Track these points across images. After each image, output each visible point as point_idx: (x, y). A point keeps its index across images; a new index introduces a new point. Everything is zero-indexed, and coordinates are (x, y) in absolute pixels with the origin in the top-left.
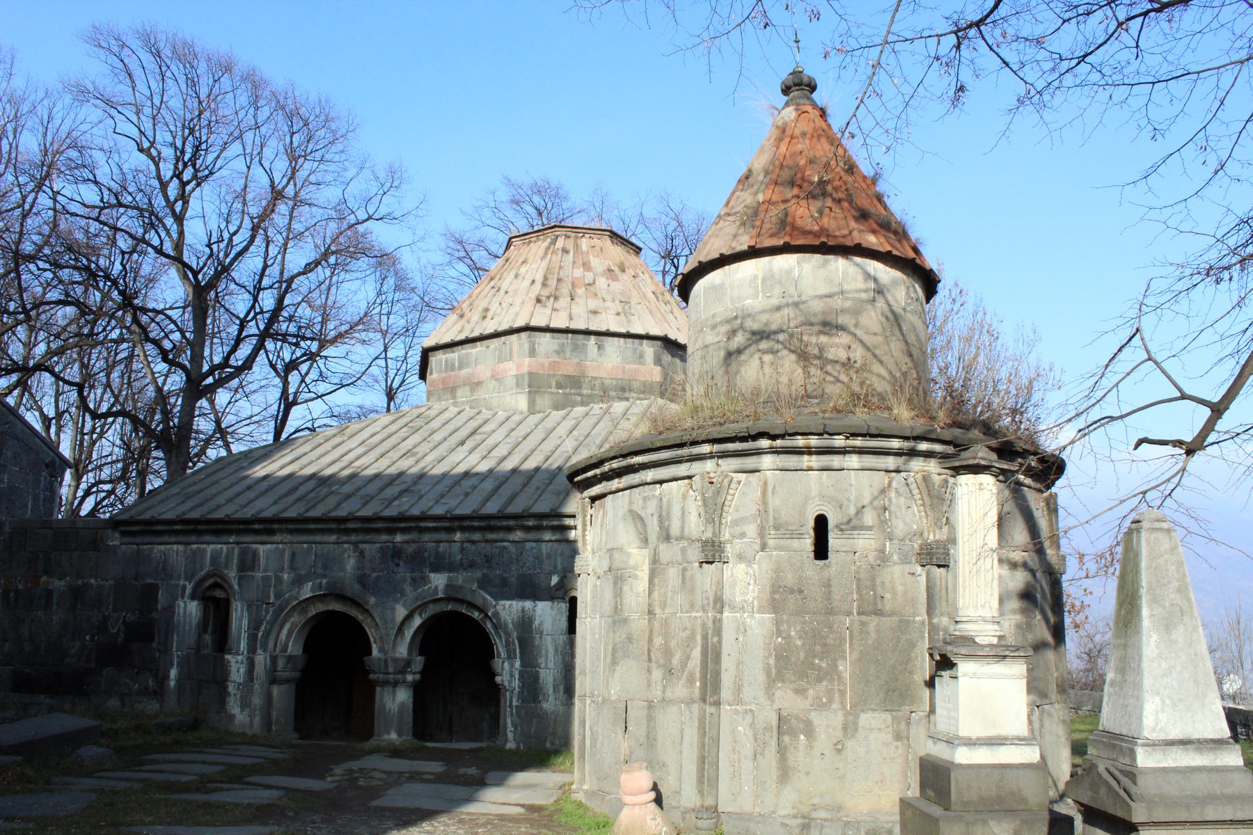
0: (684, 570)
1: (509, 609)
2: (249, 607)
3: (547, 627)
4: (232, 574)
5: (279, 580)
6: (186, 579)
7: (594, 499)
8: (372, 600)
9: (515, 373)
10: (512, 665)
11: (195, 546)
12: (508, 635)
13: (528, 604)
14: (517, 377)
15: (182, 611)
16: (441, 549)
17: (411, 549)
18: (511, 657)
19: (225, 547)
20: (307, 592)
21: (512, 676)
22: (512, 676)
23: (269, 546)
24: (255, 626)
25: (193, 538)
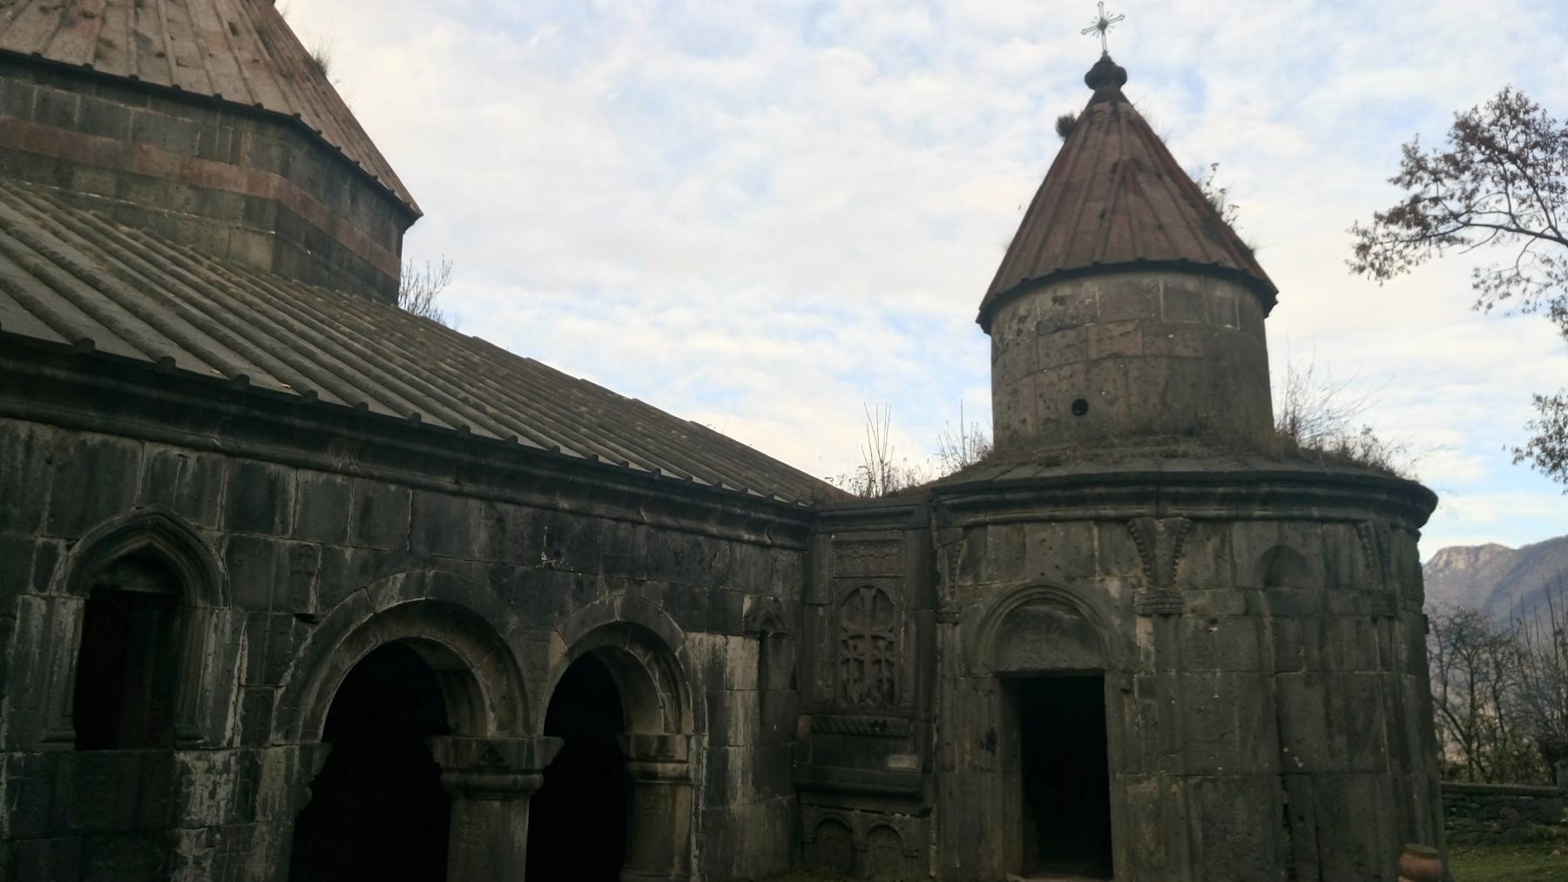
0: (1359, 623)
1: (698, 645)
2: (253, 620)
3: (738, 678)
4: (212, 531)
5: (332, 559)
6: (55, 530)
7: (1196, 520)
8: (513, 621)
9: (244, 191)
10: (699, 743)
11: (94, 439)
12: (696, 690)
13: (719, 639)
14: (248, 199)
15: (36, 622)
16: (621, 534)
17: (578, 525)
19: (192, 457)
20: (391, 596)
21: (699, 761)
22: (699, 761)
23: (309, 475)
24: (267, 667)
25: (93, 415)
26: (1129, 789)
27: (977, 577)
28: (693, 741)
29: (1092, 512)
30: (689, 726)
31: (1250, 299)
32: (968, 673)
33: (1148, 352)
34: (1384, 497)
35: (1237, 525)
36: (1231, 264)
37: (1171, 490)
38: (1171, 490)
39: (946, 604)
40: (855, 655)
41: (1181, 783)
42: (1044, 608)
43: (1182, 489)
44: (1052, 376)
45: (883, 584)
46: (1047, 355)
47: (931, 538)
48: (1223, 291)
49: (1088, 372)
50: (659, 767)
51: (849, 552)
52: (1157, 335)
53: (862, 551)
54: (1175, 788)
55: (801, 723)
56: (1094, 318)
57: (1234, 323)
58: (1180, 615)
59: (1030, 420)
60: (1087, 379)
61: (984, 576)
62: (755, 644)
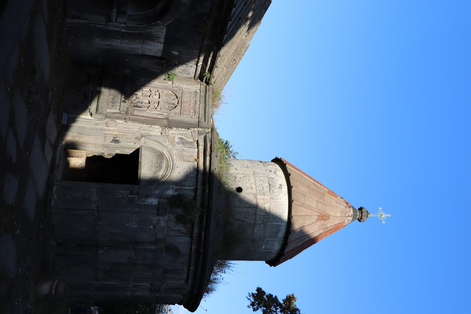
1: (161, 31)
7: (193, 225)
10: (123, 28)
13: (162, 40)
18: (128, 28)
22: (116, 27)
26: (95, 190)
27: (178, 143)
28: (124, 25)
29: (199, 187)
30: (130, 24)
31: (273, 256)
32: (142, 136)
33: (257, 216)
34: (195, 293)
35: (189, 239)
36: (286, 251)
37: (205, 217)
38: (205, 217)
39: (169, 131)
40: (152, 94)
41: (95, 208)
42: (164, 166)
43: (205, 220)
44: (252, 181)
45: (178, 108)
46: (260, 180)
47: (195, 128)
48: (277, 247)
49: (252, 193)
50: (115, 10)
51: (192, 96)
52: (263, 220)
53: (193, 101)
54: (94, 206)
55: (128, 70)
56: (272, 198)
57: (264, 249)
58: (158, 215)
59: (237, 172)
60: (250, 193)
61: (178, 146)
62: (159, 55)
